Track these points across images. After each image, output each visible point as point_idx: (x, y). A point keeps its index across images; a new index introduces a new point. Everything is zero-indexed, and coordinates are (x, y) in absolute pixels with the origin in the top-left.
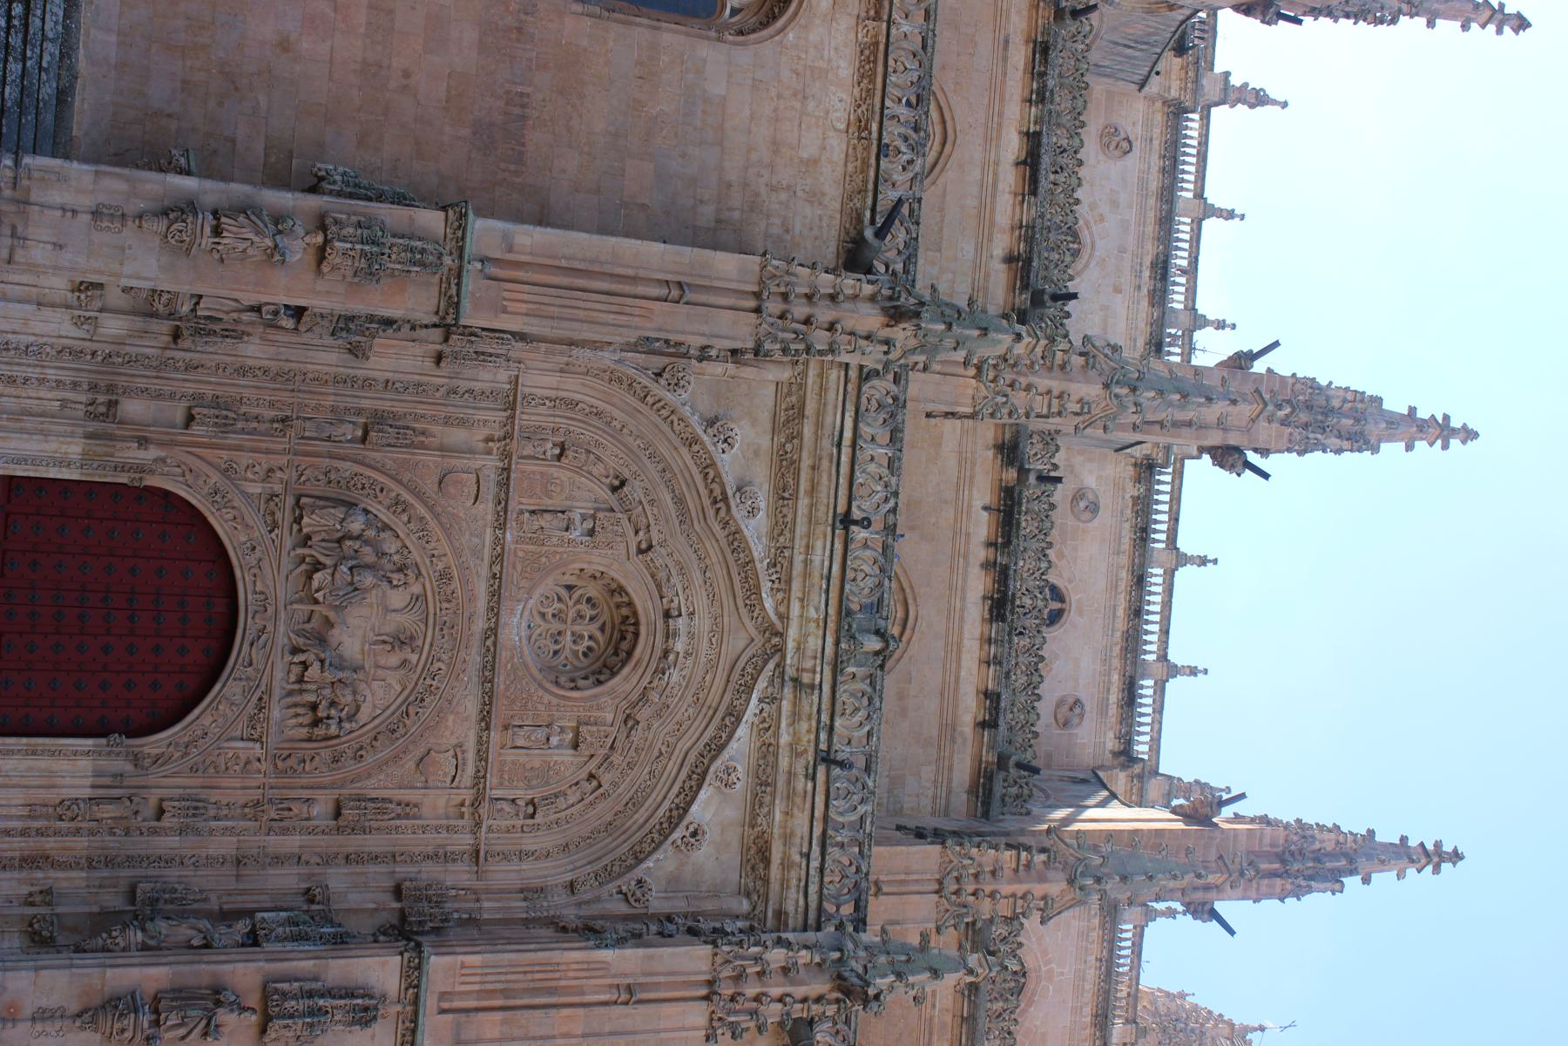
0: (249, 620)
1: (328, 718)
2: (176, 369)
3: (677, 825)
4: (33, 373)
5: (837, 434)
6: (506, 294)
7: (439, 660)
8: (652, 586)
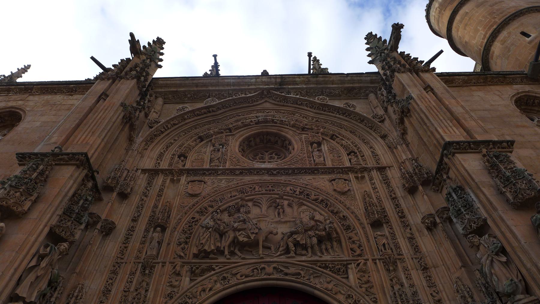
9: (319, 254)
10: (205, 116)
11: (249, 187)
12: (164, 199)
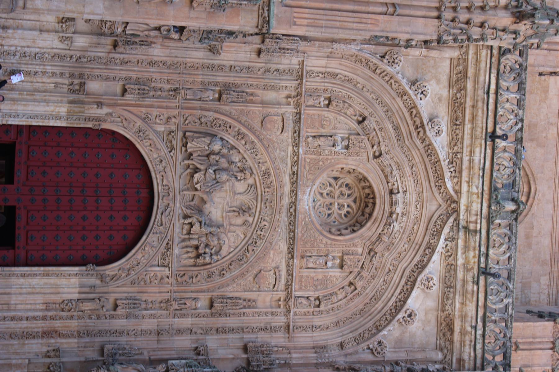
1: (205, 253)
2: (116, 64)
3: (400, 310)
4: (39, 69)
5: (486, 87)
6: (295, 15)
7: (264, 220)
8: (383, 176)
10: (410, 122)
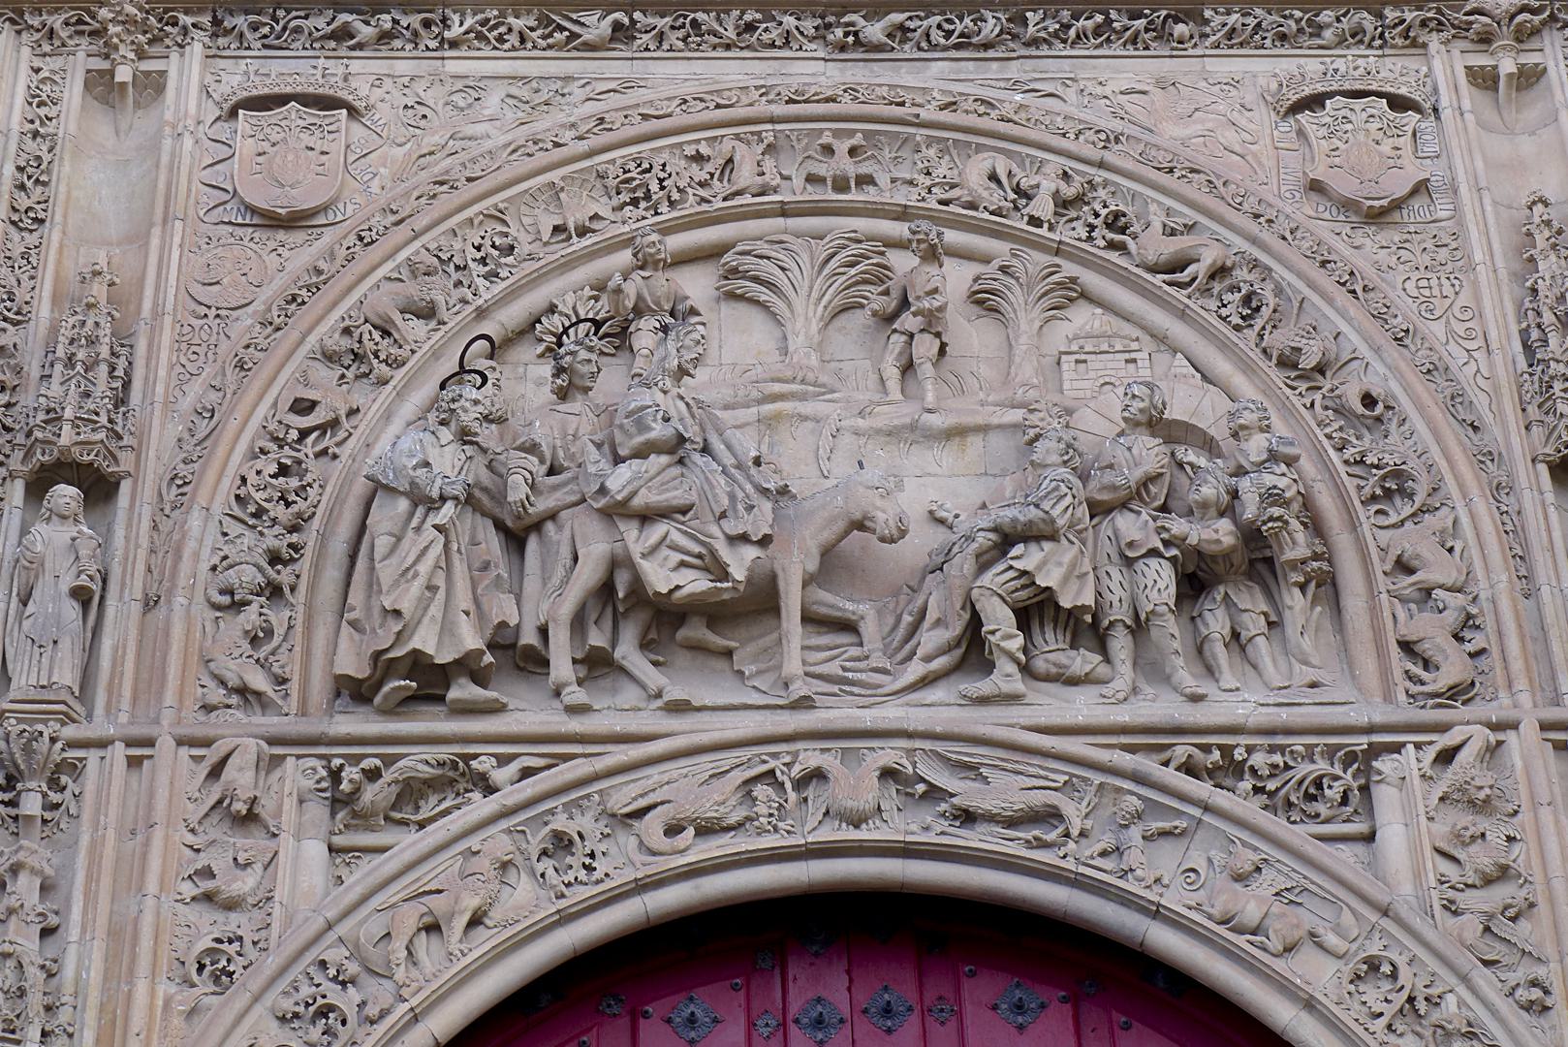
0: (863, 834)
9: (1187, 677)
11: (690, 151)
12: (61, 247)
